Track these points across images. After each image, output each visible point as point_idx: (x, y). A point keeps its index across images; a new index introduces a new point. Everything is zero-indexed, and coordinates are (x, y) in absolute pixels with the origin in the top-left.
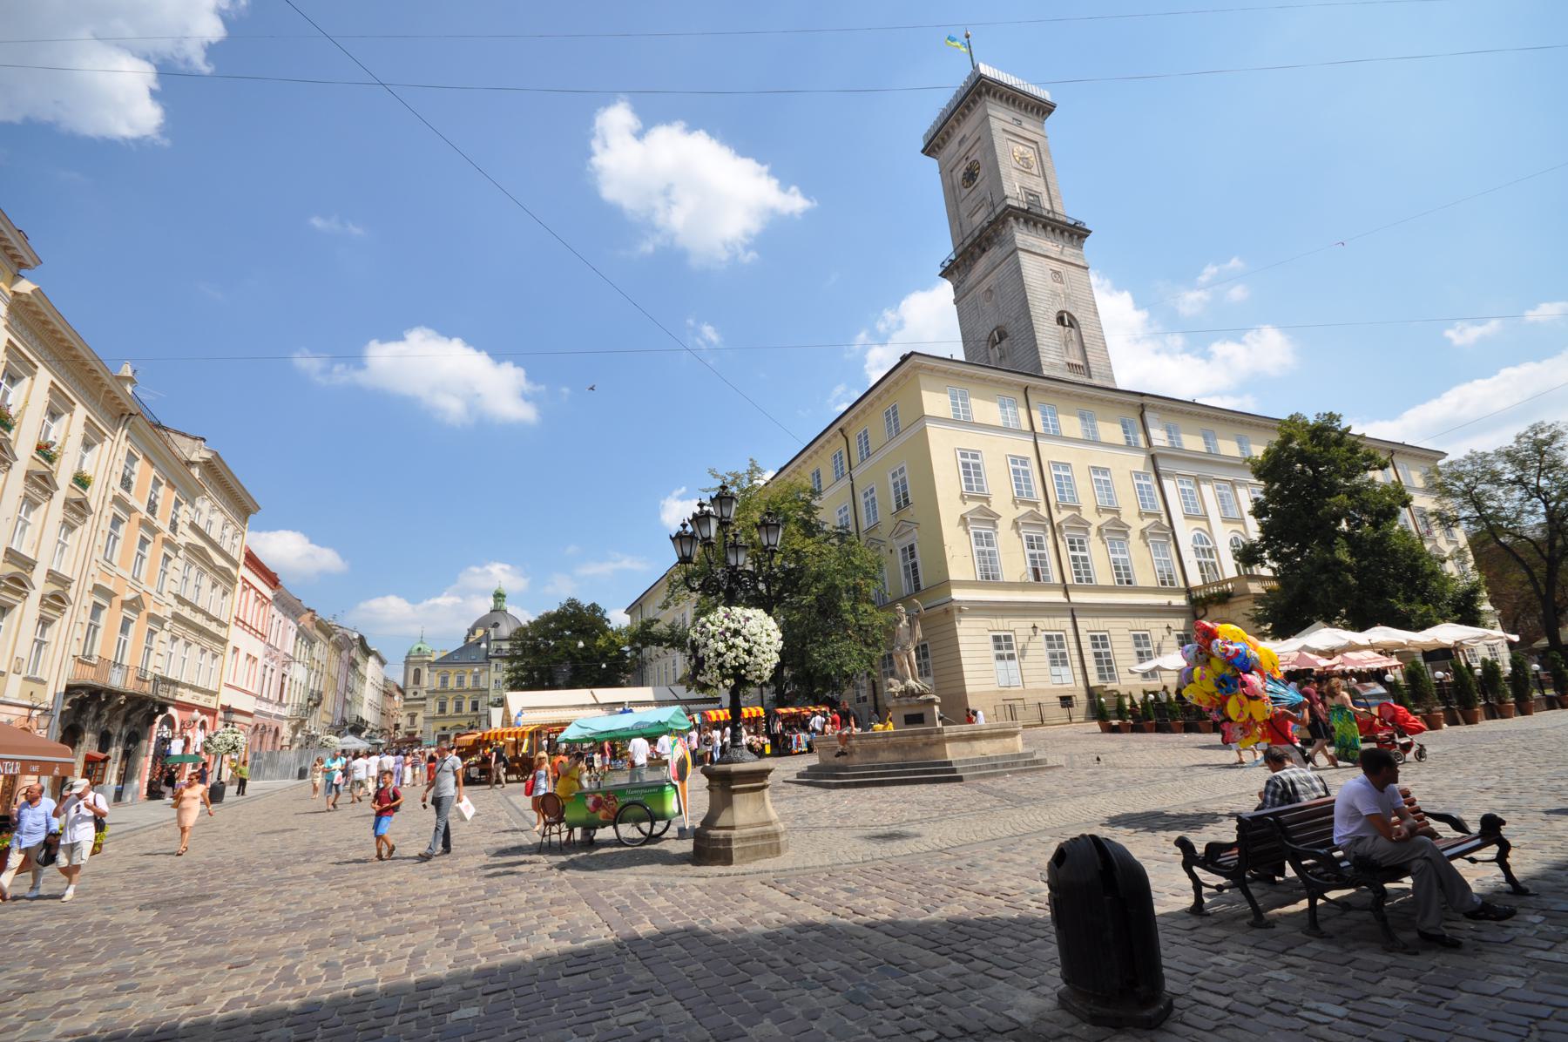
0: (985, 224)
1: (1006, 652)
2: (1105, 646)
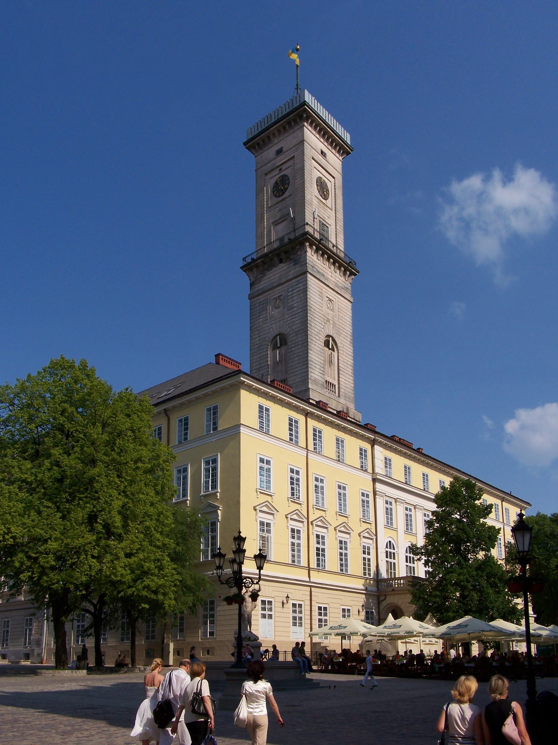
2: (326, 615)
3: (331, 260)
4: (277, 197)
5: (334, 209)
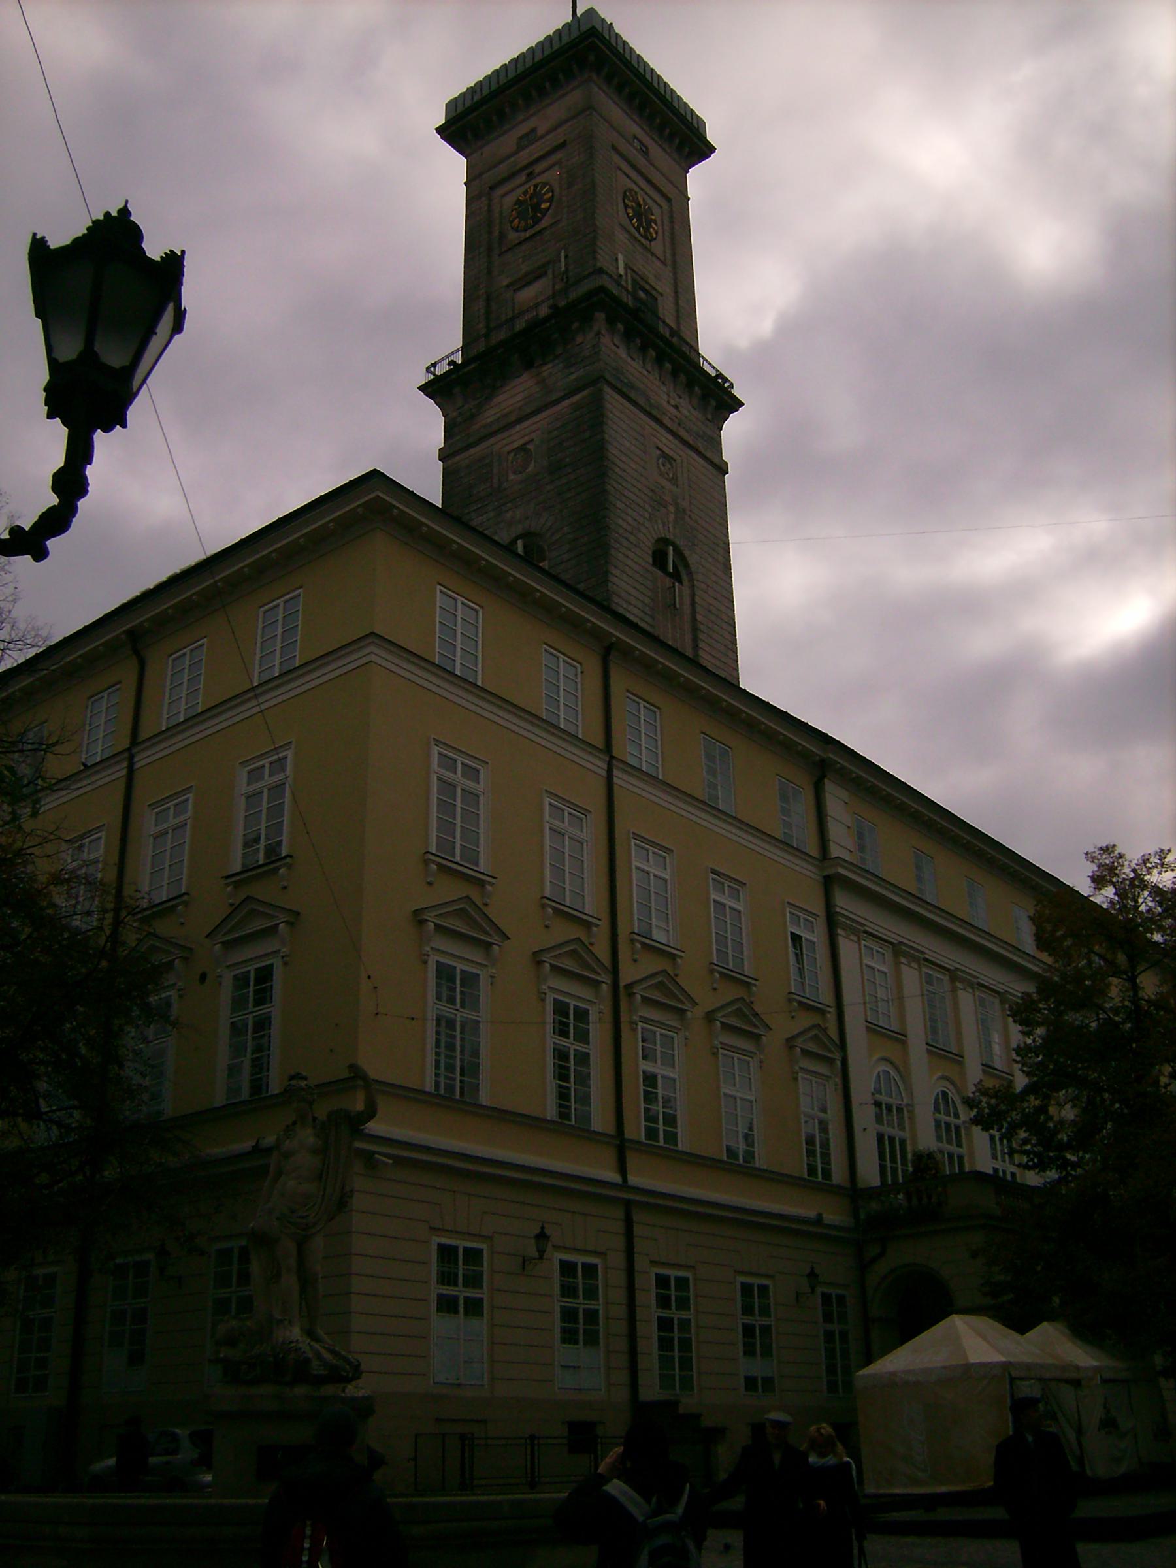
0: (544, 311)
1: (461, 1292)
2: (683, 1304)
3: (668, 366)
4: (522, 231)
5: (669, 262)
